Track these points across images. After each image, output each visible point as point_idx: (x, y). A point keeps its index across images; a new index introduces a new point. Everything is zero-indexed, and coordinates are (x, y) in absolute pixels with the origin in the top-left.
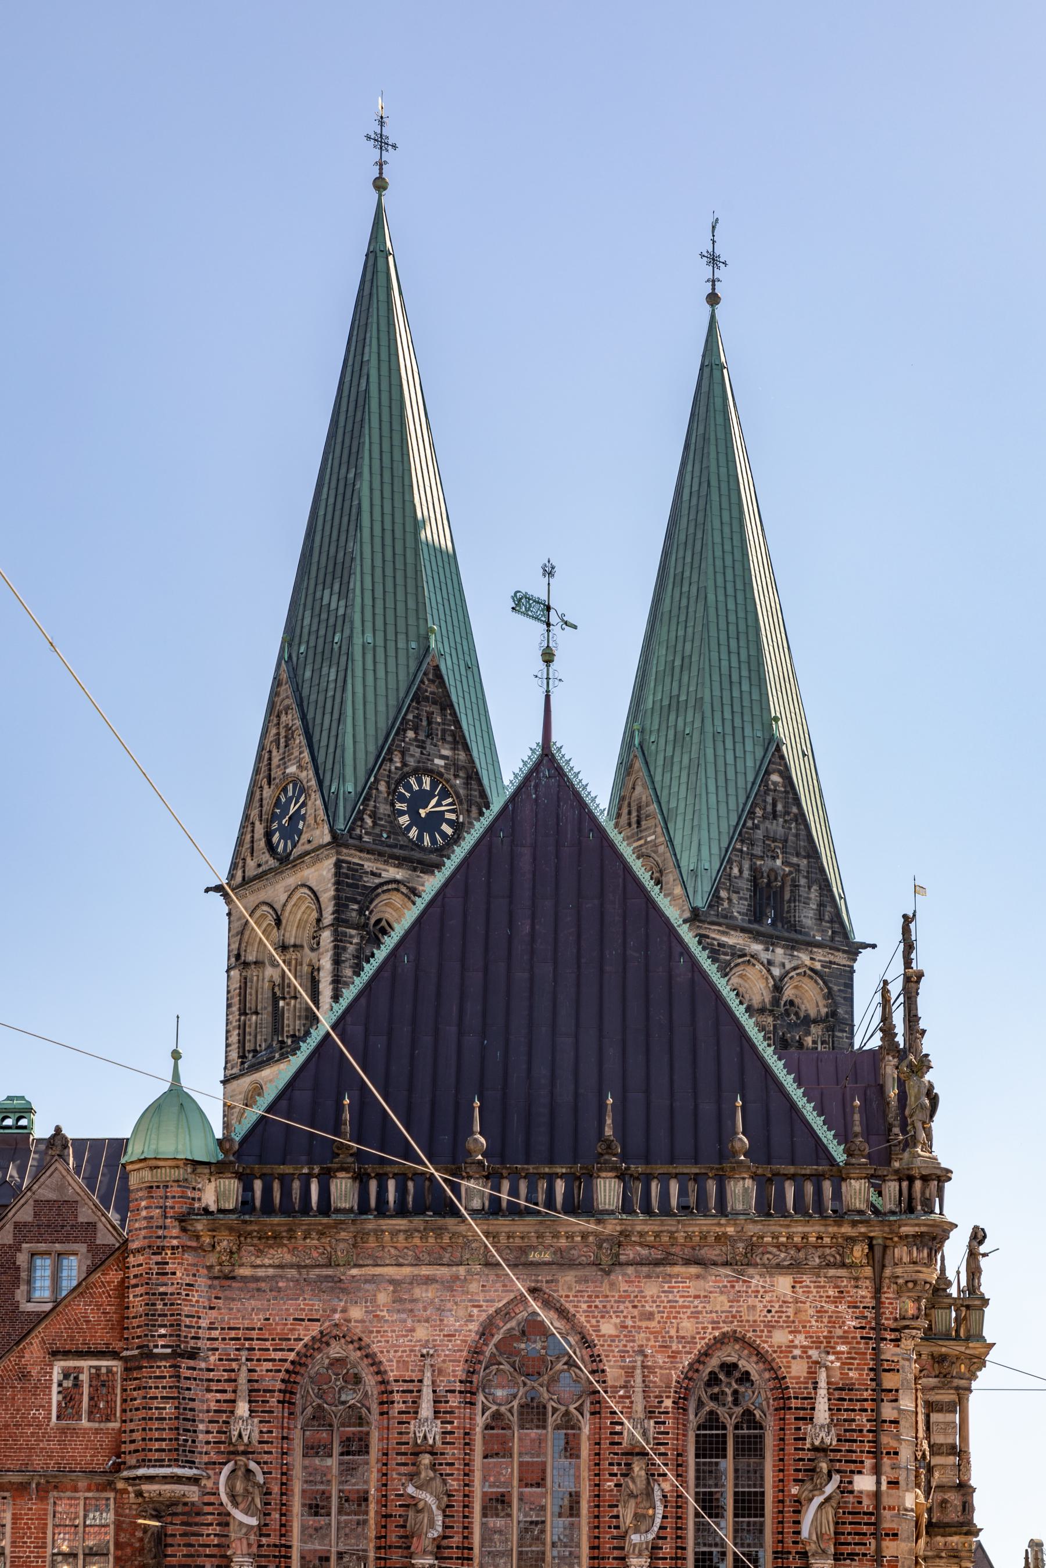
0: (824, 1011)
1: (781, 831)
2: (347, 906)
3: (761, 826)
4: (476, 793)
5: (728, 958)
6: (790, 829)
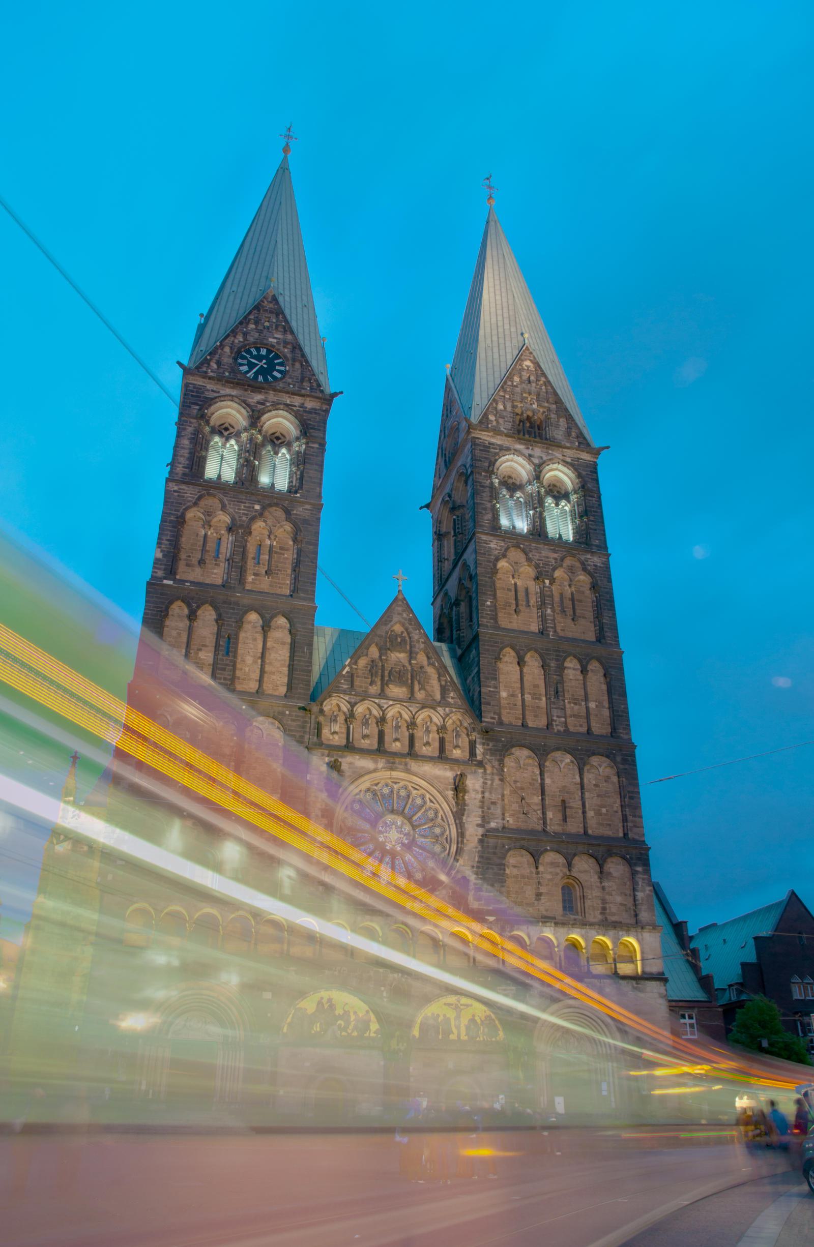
2: (190, 407)
3: (519, 386)
4: (299, 355)
5: (498, 451)
6: (542, 389)
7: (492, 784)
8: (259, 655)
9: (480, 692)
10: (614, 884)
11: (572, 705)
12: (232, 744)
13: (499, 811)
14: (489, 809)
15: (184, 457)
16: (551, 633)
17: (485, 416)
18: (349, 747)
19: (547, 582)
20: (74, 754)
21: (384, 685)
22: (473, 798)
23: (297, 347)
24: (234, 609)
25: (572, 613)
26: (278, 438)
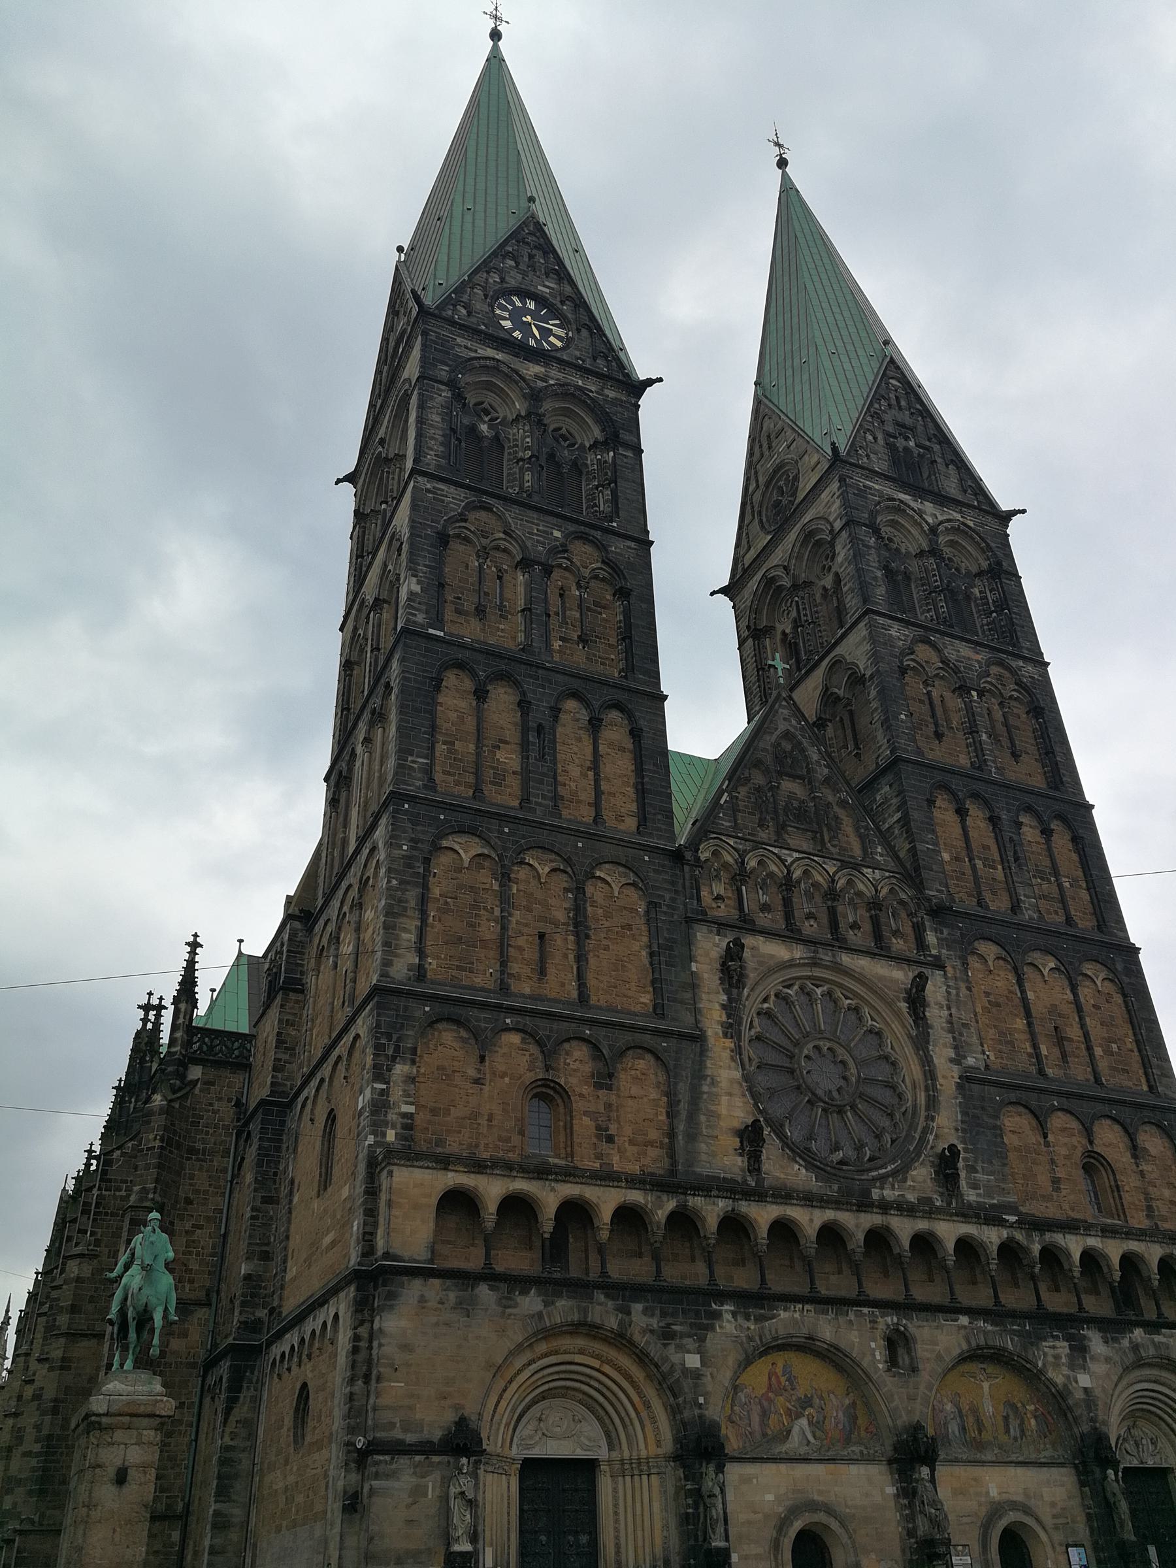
0: (985, 565)
1: (908, 421)
4: (587, 318)
7: (958, 995)
8: (588, 764)
9: (913, 851)
10: (1154, 1167)
11: (1039, 880)
12: (566, 905)
13: (975, 1040)
14: (961, 1034)
15: (435, 439)
16: (993, 770)
17: (853, 448)
18: (745, 924)
19: (974, 693)
20: (192, 939)
21: (781, 829)
22: (936, 1015)
23: (580, 303)
24: (543, 687)
25: (1009, 745)
26: (562, 436)
